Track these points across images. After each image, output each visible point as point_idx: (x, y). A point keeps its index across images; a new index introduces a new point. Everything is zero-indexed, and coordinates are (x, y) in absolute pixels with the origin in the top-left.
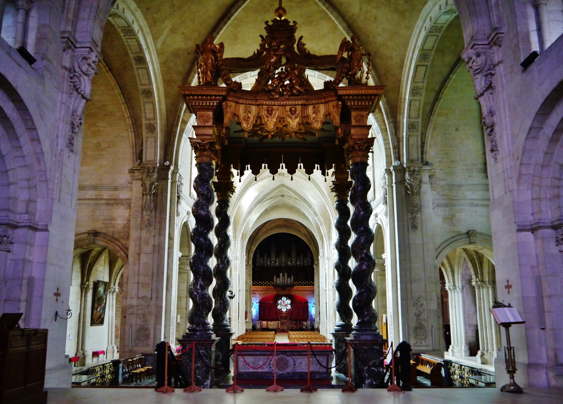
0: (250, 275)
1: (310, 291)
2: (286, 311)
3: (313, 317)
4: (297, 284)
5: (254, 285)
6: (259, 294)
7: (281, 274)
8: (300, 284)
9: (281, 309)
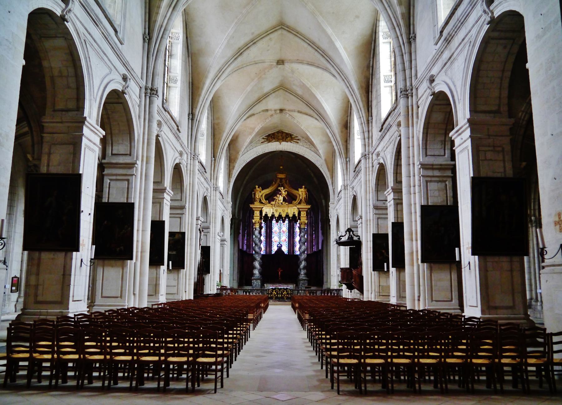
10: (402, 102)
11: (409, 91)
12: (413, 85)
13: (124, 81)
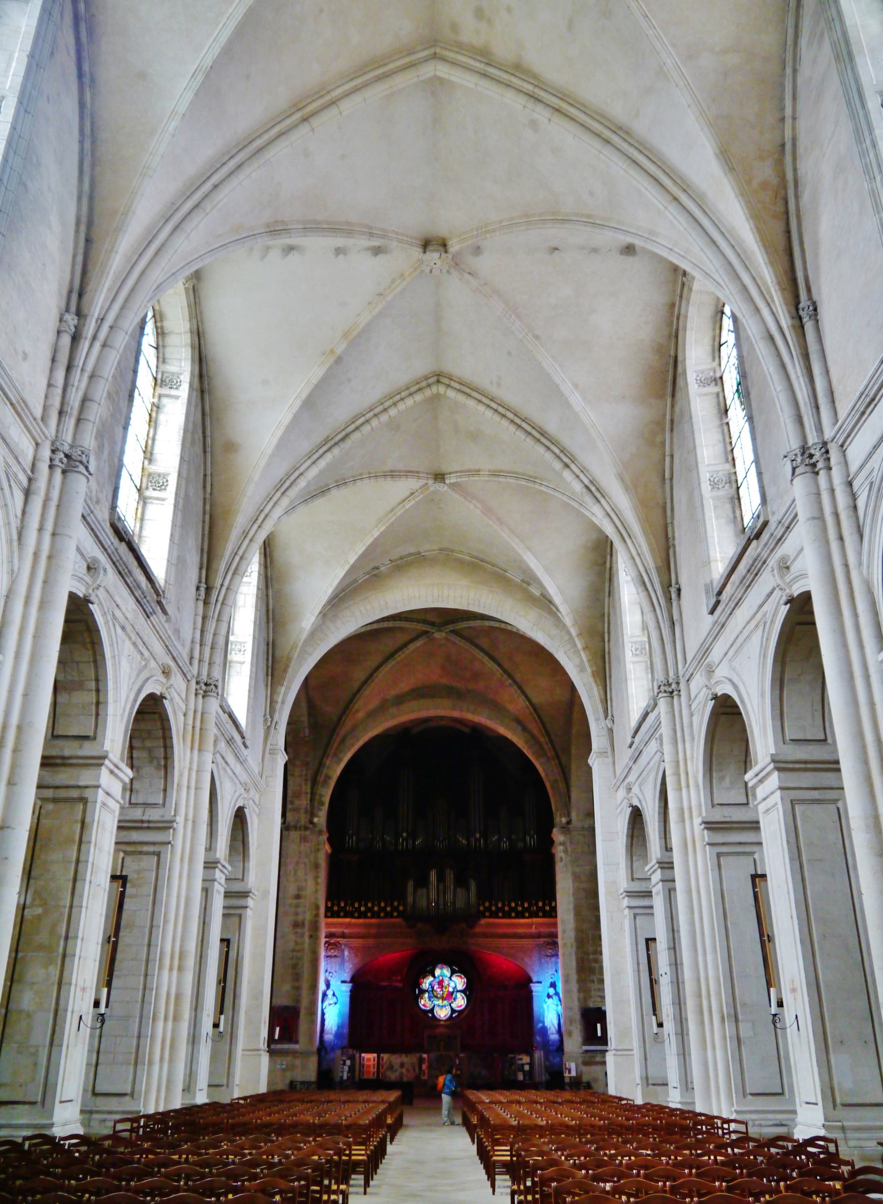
0: (317, 866)
1: (539, 936)
2: (451, 1017)
3: (554, 1036)
4: (488, 909)
5: (330, 913)
6: (351, 948)
7: (433, 876)
8: (502, 909)
9: (432, 1011)
10: (663, 704)
11: (674, 686)
12: (681, 673)
13: (166, 677)
